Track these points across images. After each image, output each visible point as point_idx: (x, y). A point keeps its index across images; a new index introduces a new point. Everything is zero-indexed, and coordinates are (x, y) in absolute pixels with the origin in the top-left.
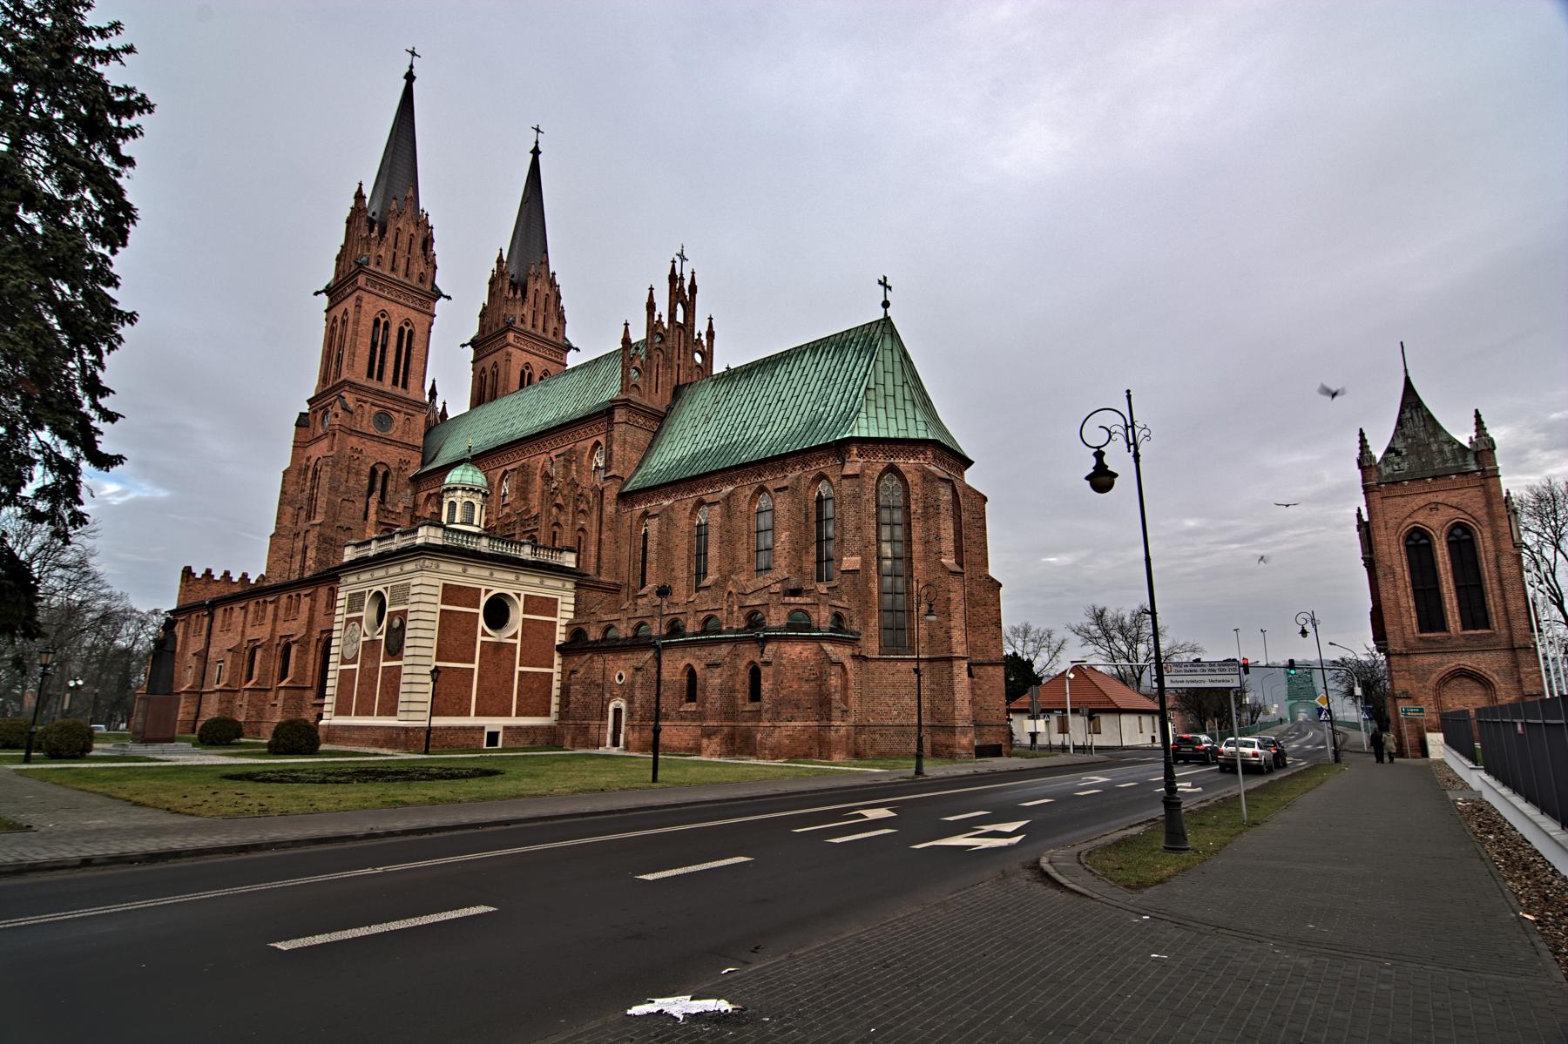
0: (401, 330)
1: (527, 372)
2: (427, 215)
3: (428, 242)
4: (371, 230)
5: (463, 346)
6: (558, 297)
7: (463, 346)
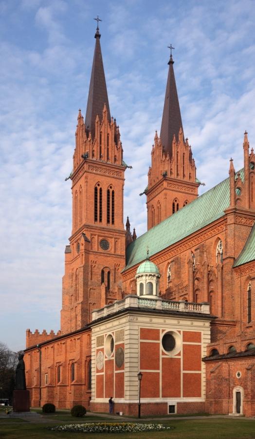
0: (108, 191)
2: (115, 120)
3: (117, 137)
4: (88, 137)
5: (141, 195)
6: (191, 154)
7: (141, 195)
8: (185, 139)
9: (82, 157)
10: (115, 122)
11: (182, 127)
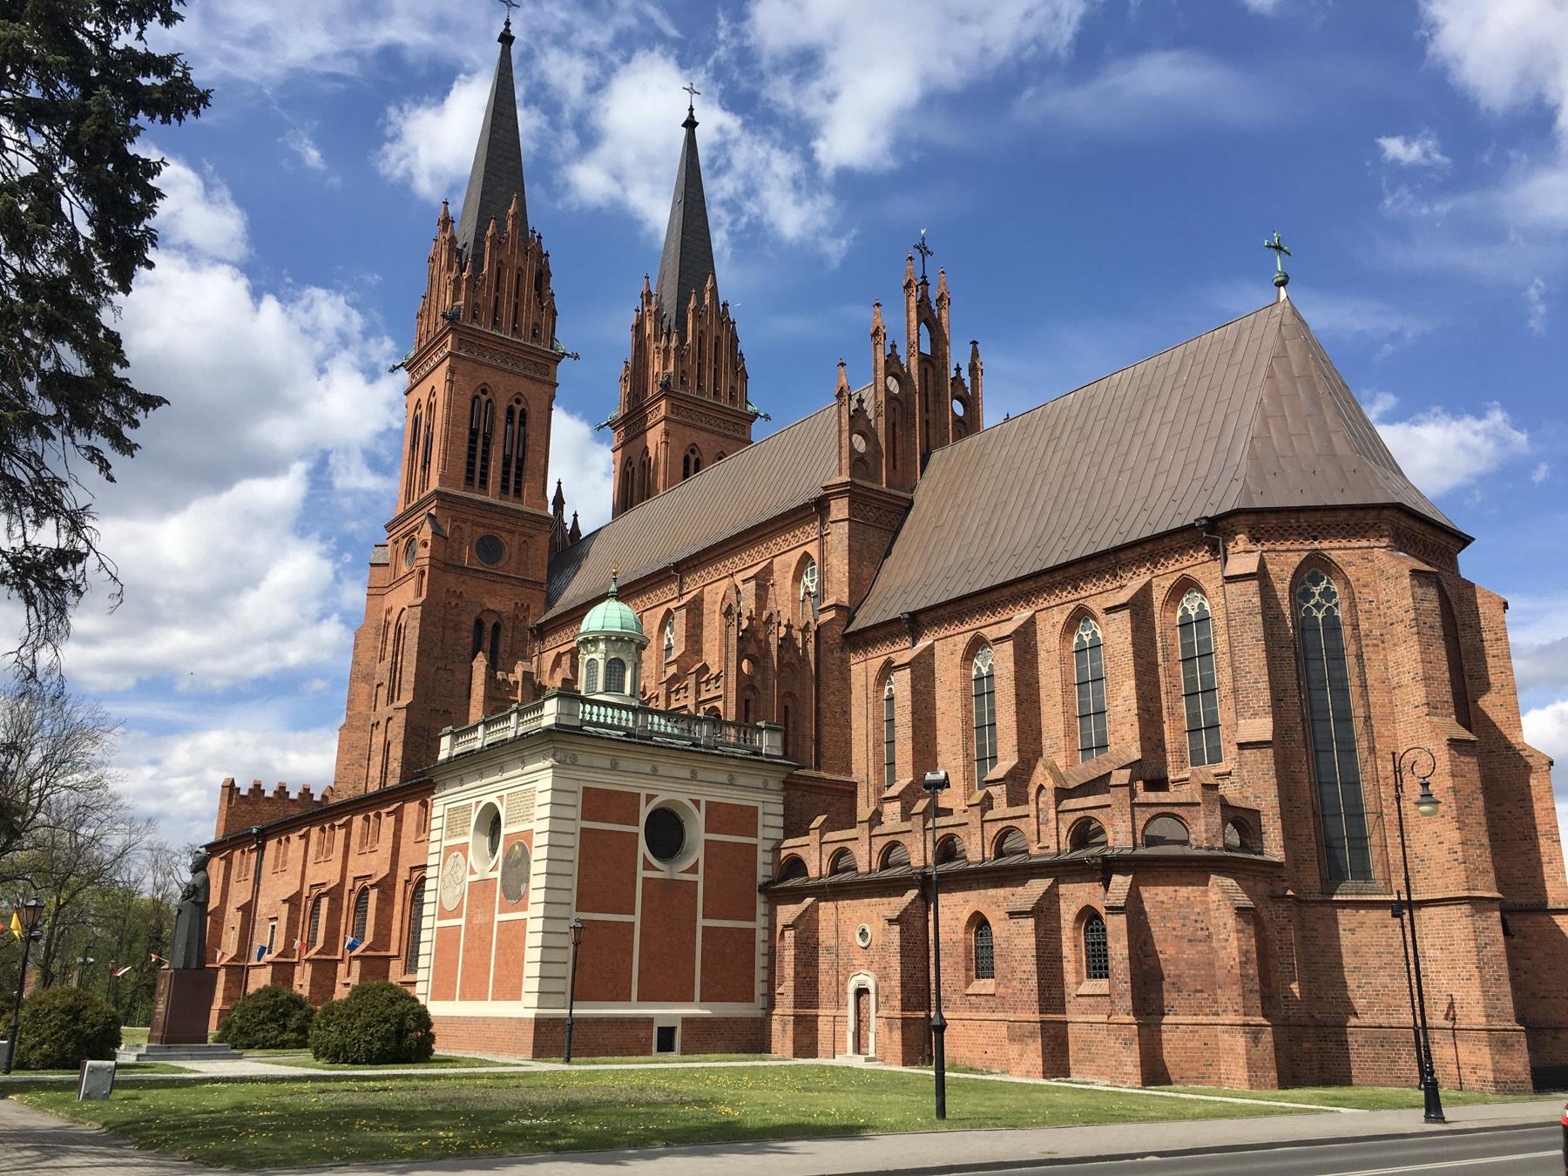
1: (693, 459)
2: (539, 237)
3: (542, 278)
6: (735, 340)
8: (721, 303)
9: (444, 316)
10: (539, 242)
11: (714, 274)
